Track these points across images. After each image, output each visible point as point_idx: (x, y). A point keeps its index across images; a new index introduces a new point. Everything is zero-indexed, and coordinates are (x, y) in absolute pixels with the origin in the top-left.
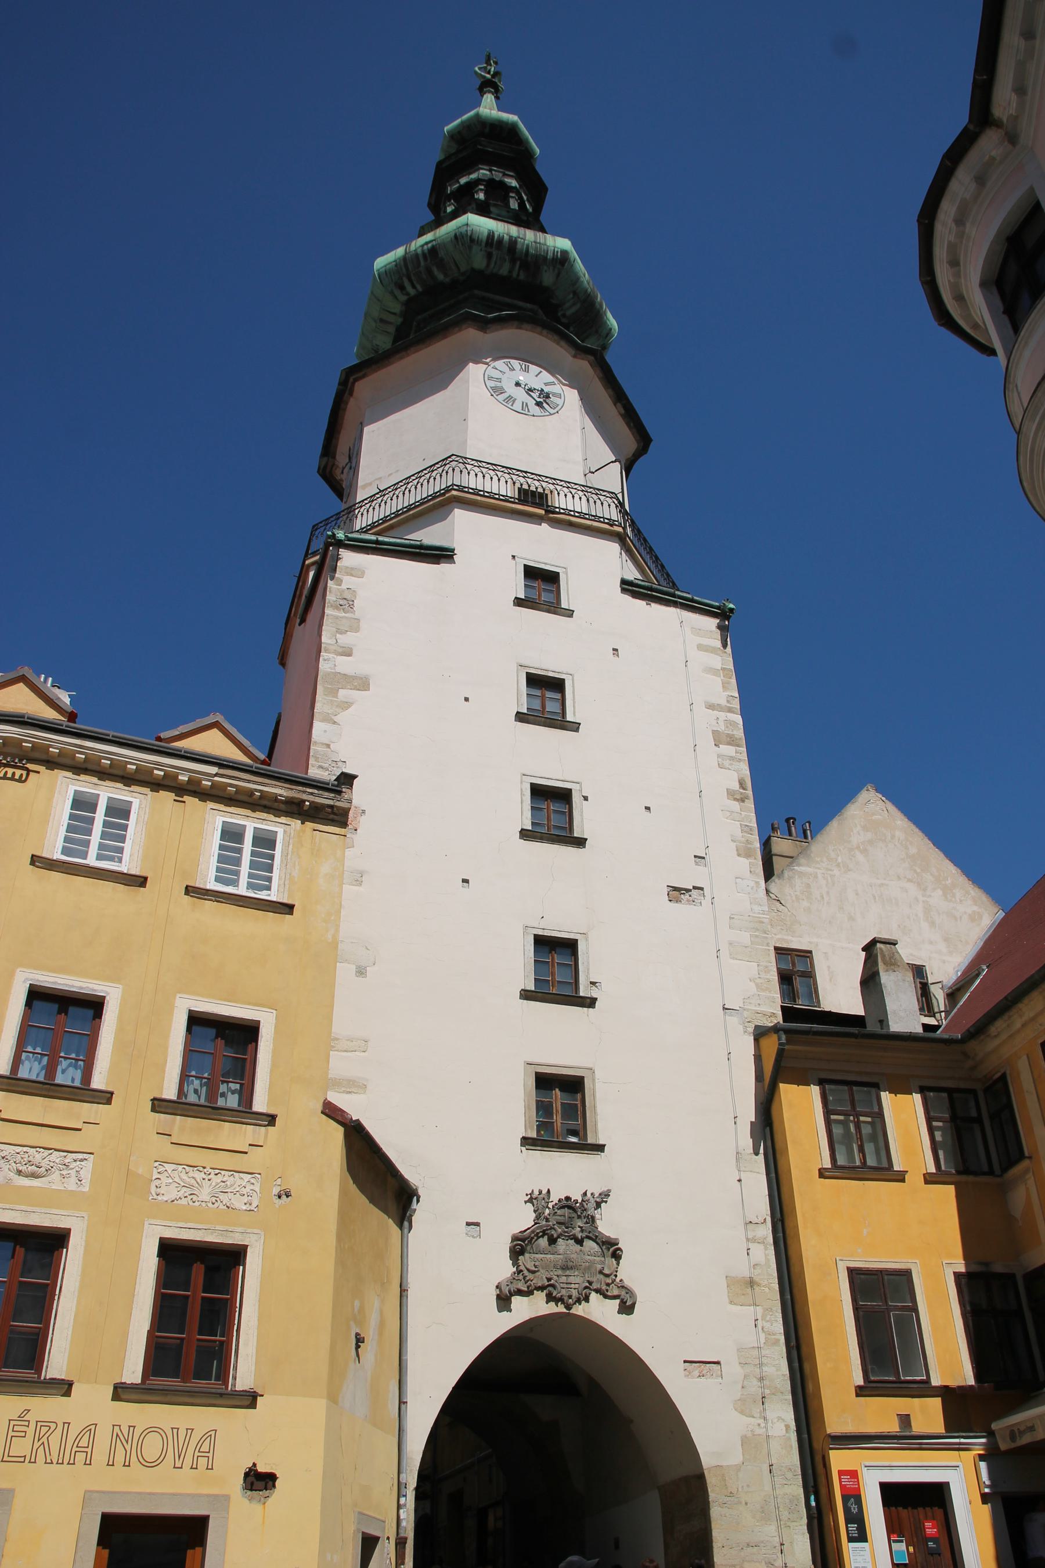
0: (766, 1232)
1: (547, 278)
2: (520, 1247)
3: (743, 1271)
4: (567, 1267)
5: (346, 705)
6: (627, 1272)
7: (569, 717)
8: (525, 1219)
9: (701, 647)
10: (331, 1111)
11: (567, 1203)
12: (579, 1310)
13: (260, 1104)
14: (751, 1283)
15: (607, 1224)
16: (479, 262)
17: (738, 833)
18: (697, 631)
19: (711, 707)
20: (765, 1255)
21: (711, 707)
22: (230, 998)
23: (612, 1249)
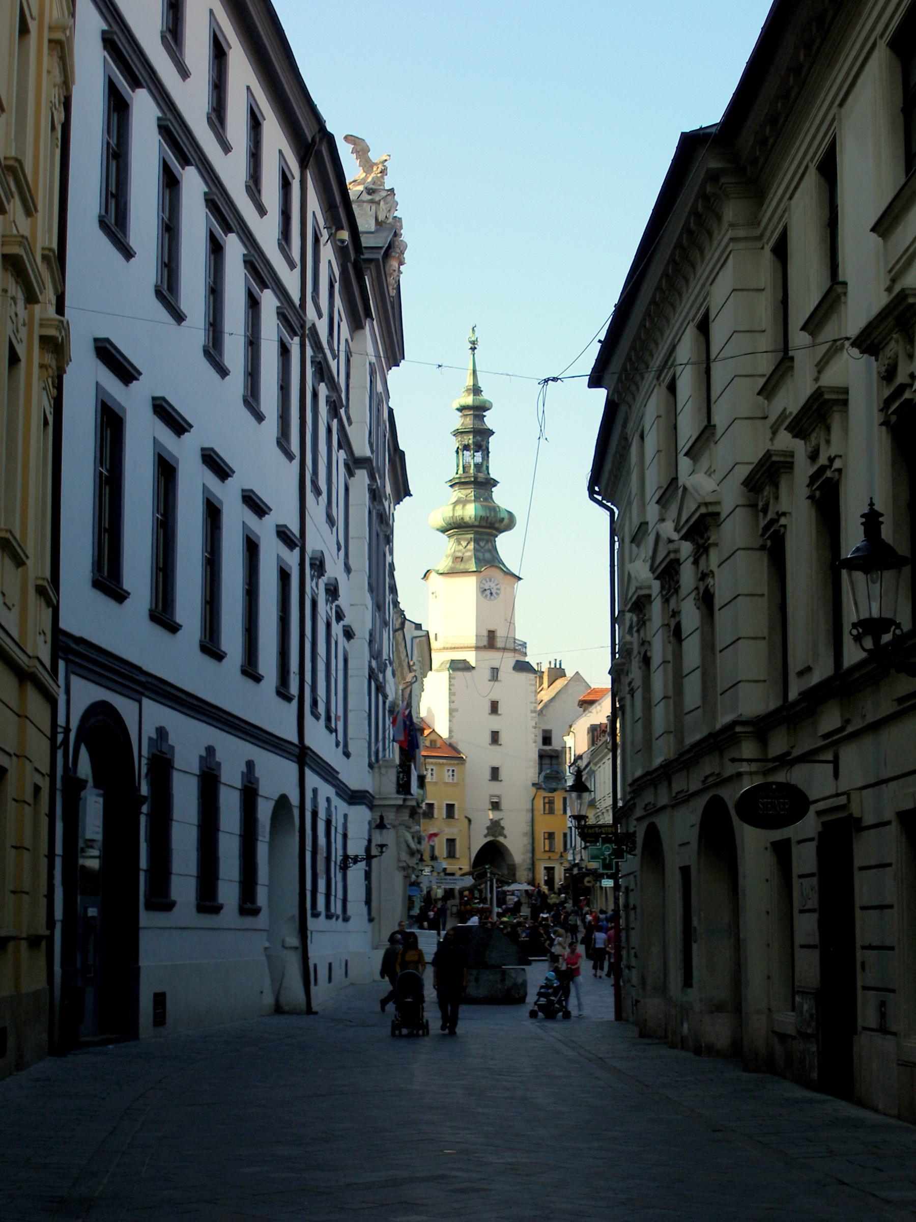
0: (530, 824)
1: (497, 525)
2: (488, 828)
3: (525, 831)
4: (496, 831)
5: (454, 717)
6: (505, 832)
7: (499, 712)
8: (488, 824)
9: (531, 685)
10: (466, 817)
11: (496, 821)
12: (498, 839)
13: (456, 817)
14: (527, 834)
15: (502, 825)
16: (477, 523)
17: (534, 737)
18: (530, 680)
19: (531, 703)
20: (529, 828)
21: (531, 703)
22: (450, 800)
23: (503, 828)
